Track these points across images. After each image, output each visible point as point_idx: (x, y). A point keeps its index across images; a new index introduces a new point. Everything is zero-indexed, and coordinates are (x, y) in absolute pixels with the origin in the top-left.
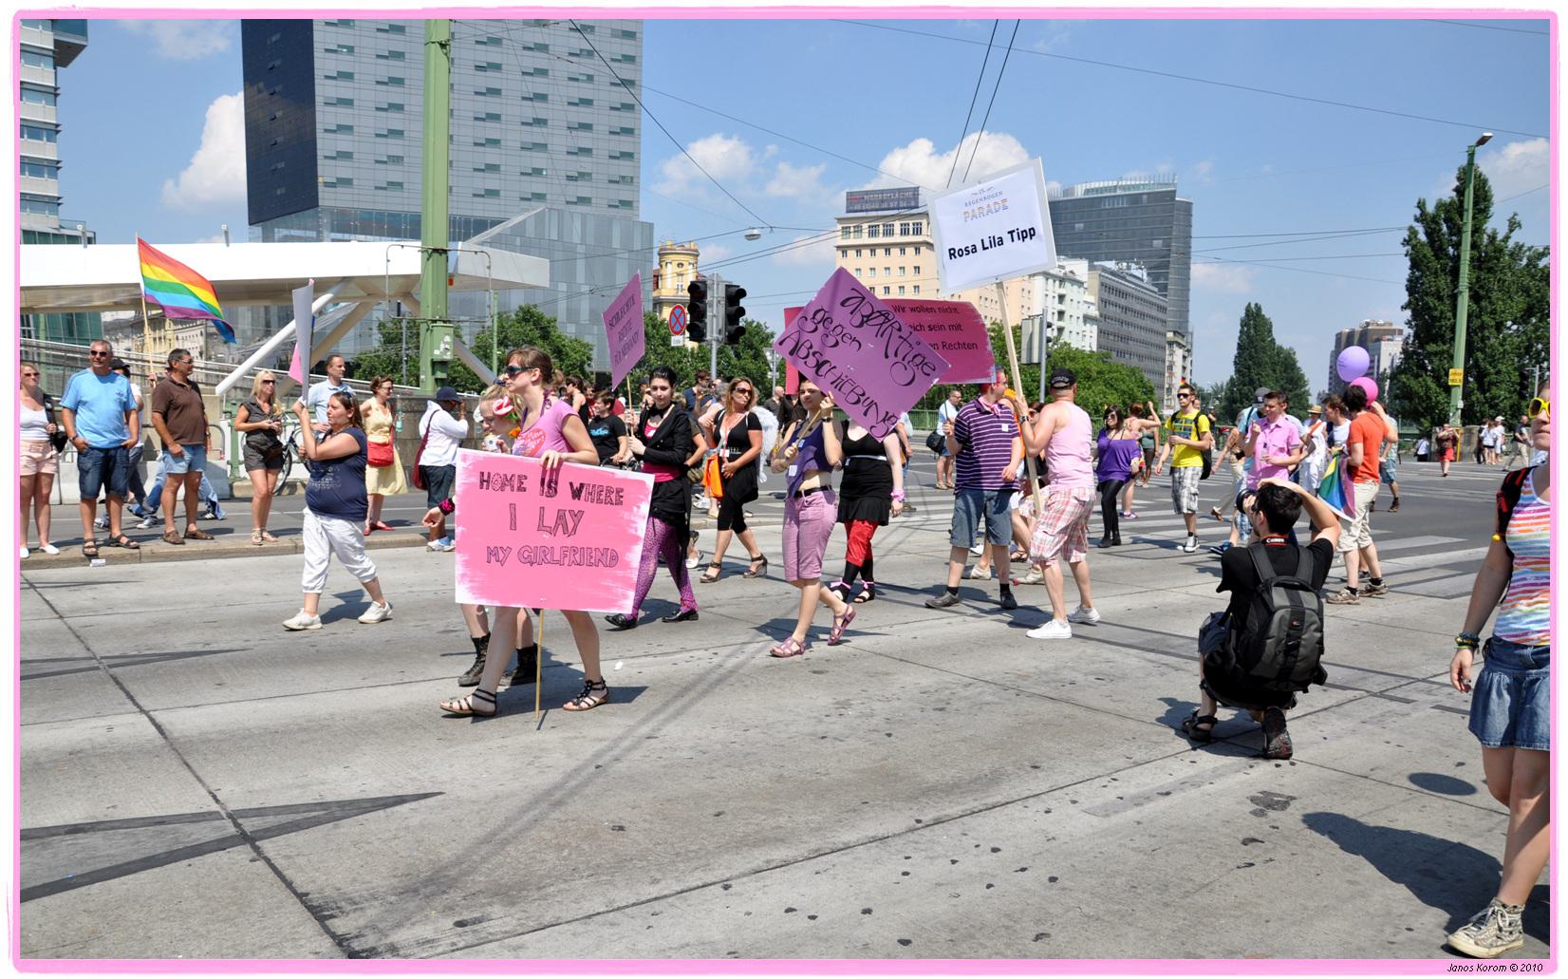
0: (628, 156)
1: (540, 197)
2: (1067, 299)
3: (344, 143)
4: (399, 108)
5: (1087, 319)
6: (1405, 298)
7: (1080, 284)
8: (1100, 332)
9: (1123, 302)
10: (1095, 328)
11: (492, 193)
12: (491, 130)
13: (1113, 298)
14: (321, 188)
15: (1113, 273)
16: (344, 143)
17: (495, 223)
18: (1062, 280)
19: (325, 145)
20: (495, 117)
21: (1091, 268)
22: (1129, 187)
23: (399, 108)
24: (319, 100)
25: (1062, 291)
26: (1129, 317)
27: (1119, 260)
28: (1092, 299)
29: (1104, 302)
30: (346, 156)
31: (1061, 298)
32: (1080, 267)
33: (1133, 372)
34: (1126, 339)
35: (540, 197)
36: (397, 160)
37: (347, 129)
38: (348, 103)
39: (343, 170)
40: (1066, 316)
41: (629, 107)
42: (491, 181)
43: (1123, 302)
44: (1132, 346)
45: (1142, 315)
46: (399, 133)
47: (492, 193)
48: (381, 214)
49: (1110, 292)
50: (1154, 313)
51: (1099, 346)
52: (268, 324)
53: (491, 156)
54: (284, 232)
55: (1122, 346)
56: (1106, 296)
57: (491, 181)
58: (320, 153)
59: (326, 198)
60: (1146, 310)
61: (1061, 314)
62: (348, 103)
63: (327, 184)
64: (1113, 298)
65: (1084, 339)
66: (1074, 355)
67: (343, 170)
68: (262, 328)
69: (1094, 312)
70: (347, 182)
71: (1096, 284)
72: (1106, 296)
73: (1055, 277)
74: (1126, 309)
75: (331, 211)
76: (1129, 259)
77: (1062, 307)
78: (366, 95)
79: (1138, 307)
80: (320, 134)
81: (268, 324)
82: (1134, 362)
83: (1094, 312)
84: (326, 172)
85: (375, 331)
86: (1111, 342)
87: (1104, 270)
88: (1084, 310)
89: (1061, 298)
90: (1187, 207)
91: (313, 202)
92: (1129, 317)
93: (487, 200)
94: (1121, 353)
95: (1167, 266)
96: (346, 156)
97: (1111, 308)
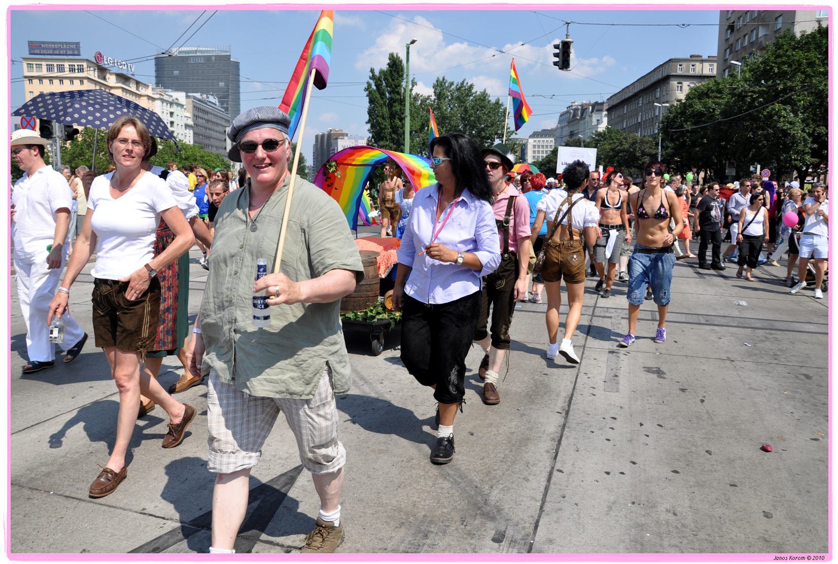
2: (175, 114)
5: (187, 126)
6: (367, 117)
7: (182, 106)
8: (195, 134)
9: (206, 117)
10: (191, 132)
13: (200, 115)
15: (199, 100)
18: (171, 104)
21: (187, 97)
22: (207, 51)
25: (172, 110)
26: (210, 125)
27: (202, 93)
28: (189, 115)
29: (196, 117)
31: (172, 114)
32: (181, 96)
33: (218, 156)
34: (209, 137)
40: (175, 124)
43: (206, 117)
44: (212, 142)
45: (217, 124)
49: (199, 110)
50: (223, 123)
51: (195, 142)
55: (207, 141)
56: (196, 113)
60: (219, 121)
61: (172, 123)
64: (200, 115)
65: (186, 137)
66: (185, 147)
69: (190, 122)
71: (191, 107)
72: (196, 113)
73: (167, 102)
74: (208, 121)
76: (207, 93)
77: (172, 119)
79: (214, 120)
82: (214, 151)
83: (190, 122)
86: (201, 139)
87: (195, 98)
88: (185, 121)
89: (172, 114)
90: (237, 65)
92: (210, 125)
94: (208, 146)
95: (226, 96)
97: (200, 120)
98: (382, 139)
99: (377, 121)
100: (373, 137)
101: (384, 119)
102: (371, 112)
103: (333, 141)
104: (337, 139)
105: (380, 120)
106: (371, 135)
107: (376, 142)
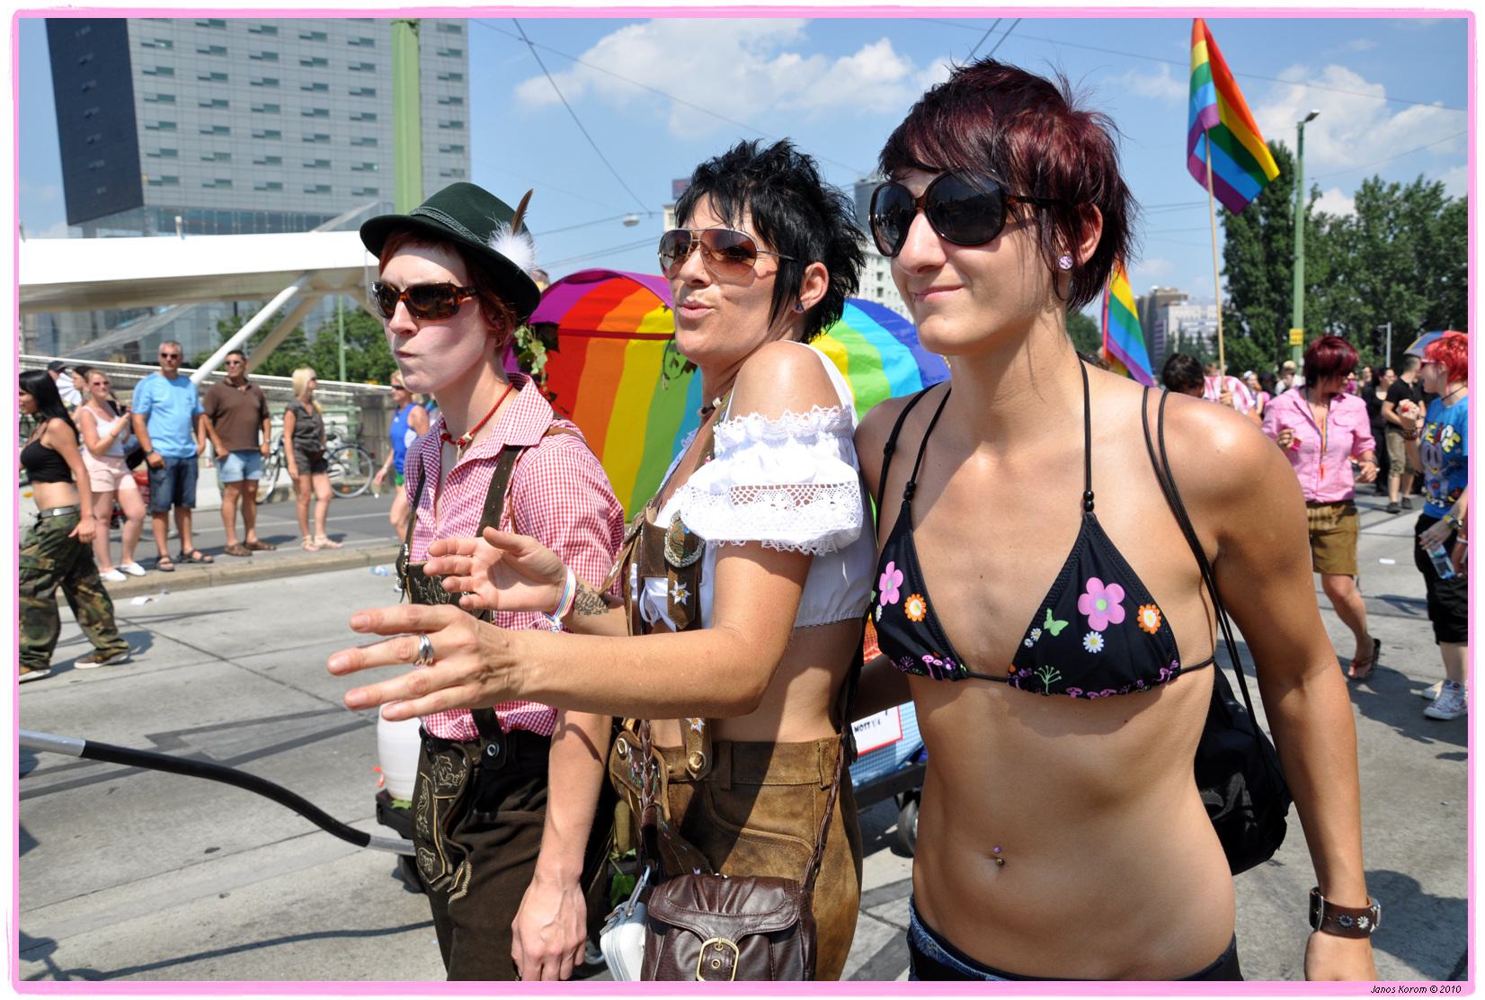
0: (458, 149)
1: (372, 192)
3: (166, 140)
4: (223, 104)
11: (323, 189)
12: (320, 125)
14: (145, 187)
16: (166, 140)
17: (327, 219)
19: (148, 141)
20: (322, 113)
23: (223, 104)
24: (138, 96)
30: (171, 153)
35: (372, 192)
36: (223, 157)
37: (170, 126)
38: (169, 99)
39: (168, 168)
41: (457, 101)
42: (322, 177)
46: (223, 130)
47: (323, 189)
48: (210, 213)
52: (94, 327)
53: (321, 151)
54: (108, 232)
57: (322, 177)
58: (142, 151)
59: (151, 196)
61: (880, 290)
62: (169, 99)
63: (152, 183)
67: (168, 168)
68: (90, 330)
70: (172, 180)
75: (158, 211)
77: (880, 284)
78: (188, 90)
80: (141, 131)
81: (94, 327)
84: (149, 169)
85: (214, 331)
91: (136, 200)
93: (319, 196)
96: (171, 153)
98: (1250, 302)
99: (1241, 270)
100: (1233, 300)
101: (1254, 264)
102: (1229, 255)
103: (1159, 311)
104: (1166, 305)
105: (1247, 267)
106: (1229, 297)
107: (1239, 308)
